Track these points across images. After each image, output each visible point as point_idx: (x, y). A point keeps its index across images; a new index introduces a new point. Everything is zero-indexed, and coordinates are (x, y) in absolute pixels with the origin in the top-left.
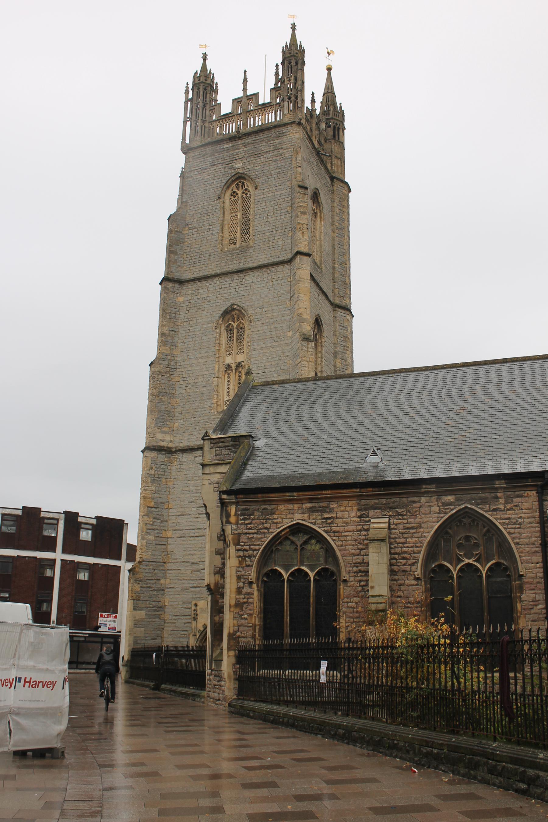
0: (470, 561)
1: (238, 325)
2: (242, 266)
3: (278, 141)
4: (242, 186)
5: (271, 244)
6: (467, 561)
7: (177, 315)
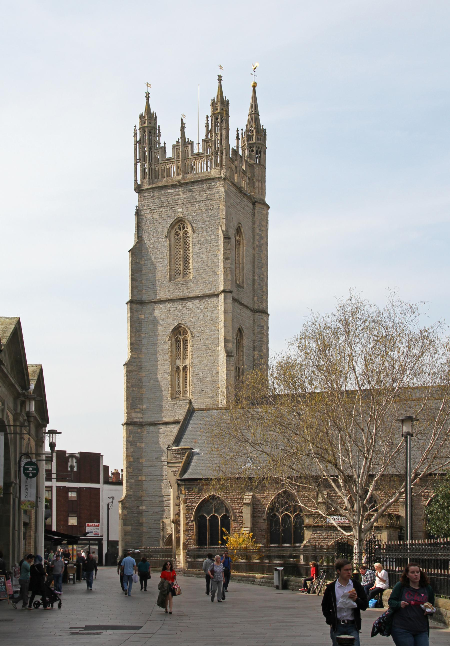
0: (287, 513)
1: (184, 338)
2: (185, 295)
3: (209, 192)
4: (183, 227)
5: (205, 279)
6: (286, 513)
7: (140, 328)
